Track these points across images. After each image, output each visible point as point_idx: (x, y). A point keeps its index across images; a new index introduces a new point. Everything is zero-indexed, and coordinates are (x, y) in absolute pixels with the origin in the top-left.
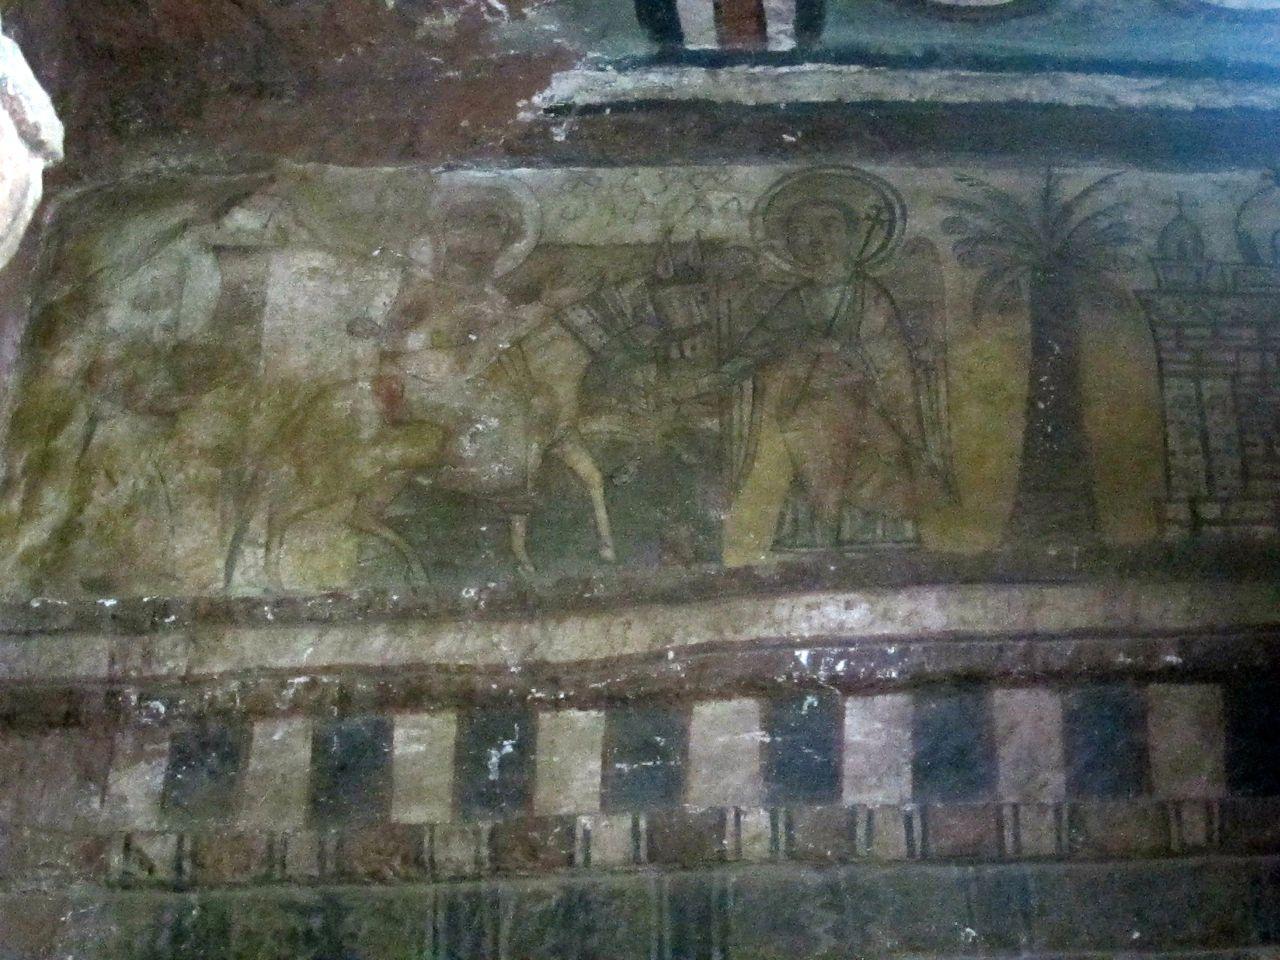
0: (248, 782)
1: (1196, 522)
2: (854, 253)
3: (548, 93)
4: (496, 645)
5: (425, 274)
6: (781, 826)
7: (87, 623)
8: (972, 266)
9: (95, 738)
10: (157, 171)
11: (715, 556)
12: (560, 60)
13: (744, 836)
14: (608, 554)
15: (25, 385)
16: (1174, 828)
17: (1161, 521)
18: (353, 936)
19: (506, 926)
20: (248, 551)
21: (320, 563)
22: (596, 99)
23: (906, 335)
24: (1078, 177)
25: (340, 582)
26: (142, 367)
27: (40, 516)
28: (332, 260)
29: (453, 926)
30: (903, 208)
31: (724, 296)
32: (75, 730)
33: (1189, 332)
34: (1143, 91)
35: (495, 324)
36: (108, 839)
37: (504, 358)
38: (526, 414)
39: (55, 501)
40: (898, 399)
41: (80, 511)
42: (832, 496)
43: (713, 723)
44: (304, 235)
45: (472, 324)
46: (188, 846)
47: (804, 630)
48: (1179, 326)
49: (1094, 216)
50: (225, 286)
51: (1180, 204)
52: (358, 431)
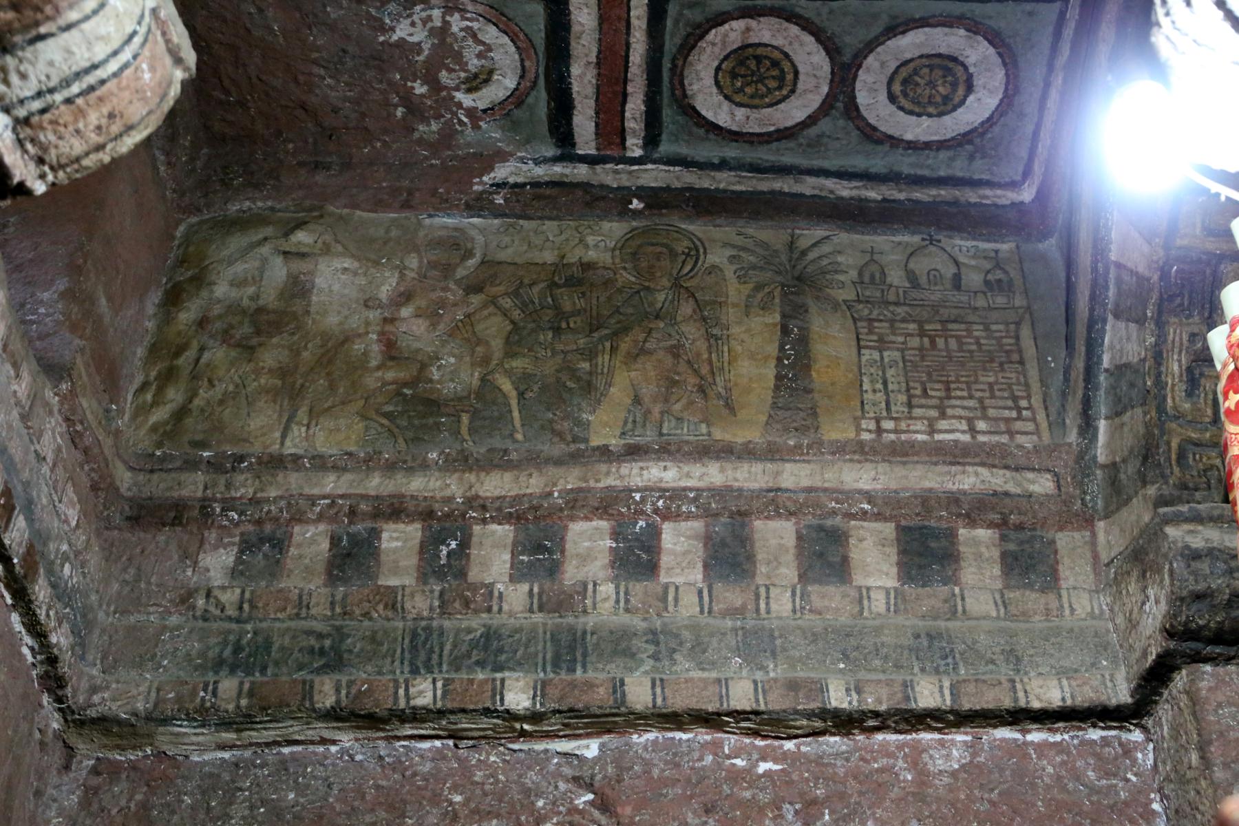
0: (288, 561)
1: (879, 431)
2: (675, 272)
3: (492, 175)
4: (448, 486)
5: (413, 275)
6: (622, 594)
7: (192, 465)
8: (745, 283)
9: (191, 533)
10: (250, 209)
11: (586, 440)
12: (502, 156)
13: (598, 599)
14: (519, 437)
15: (159, 328)
16: (866, 602)
17: (859, 429)
18: (350, 651)
19: (448, 647)
20: (295, 428)
21: (342, 436)
22: (520, 180)
23: (704, 319)
24: (810, 234)
25: (353, 449)
26: (235, 320)
27: (165, 404)
28: (356, 264)
29: (414, 648)
30: (705, 249)
31: (595, 295)
32: (179, 529)
33: (876, 324)
34: (851, 189)
35: (455, 305)
36: (196, 590)
37: (460, 324)
38: (472, 356)
39: (175, 396)
40: (698, 355)
41: (190, 402)
42: (656, 410)
43: (581, 534)
44: (340, 248)
45: (442, 304)
46: (247, 595)
47: (637, 481)
48: (871, 320)
49: (820, 258)
50: (289, 275)
51: (872, 253)
52: (368, 362)
